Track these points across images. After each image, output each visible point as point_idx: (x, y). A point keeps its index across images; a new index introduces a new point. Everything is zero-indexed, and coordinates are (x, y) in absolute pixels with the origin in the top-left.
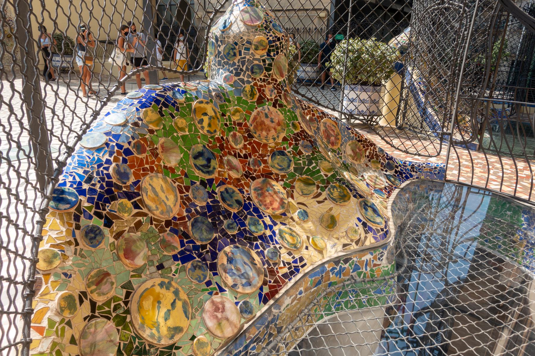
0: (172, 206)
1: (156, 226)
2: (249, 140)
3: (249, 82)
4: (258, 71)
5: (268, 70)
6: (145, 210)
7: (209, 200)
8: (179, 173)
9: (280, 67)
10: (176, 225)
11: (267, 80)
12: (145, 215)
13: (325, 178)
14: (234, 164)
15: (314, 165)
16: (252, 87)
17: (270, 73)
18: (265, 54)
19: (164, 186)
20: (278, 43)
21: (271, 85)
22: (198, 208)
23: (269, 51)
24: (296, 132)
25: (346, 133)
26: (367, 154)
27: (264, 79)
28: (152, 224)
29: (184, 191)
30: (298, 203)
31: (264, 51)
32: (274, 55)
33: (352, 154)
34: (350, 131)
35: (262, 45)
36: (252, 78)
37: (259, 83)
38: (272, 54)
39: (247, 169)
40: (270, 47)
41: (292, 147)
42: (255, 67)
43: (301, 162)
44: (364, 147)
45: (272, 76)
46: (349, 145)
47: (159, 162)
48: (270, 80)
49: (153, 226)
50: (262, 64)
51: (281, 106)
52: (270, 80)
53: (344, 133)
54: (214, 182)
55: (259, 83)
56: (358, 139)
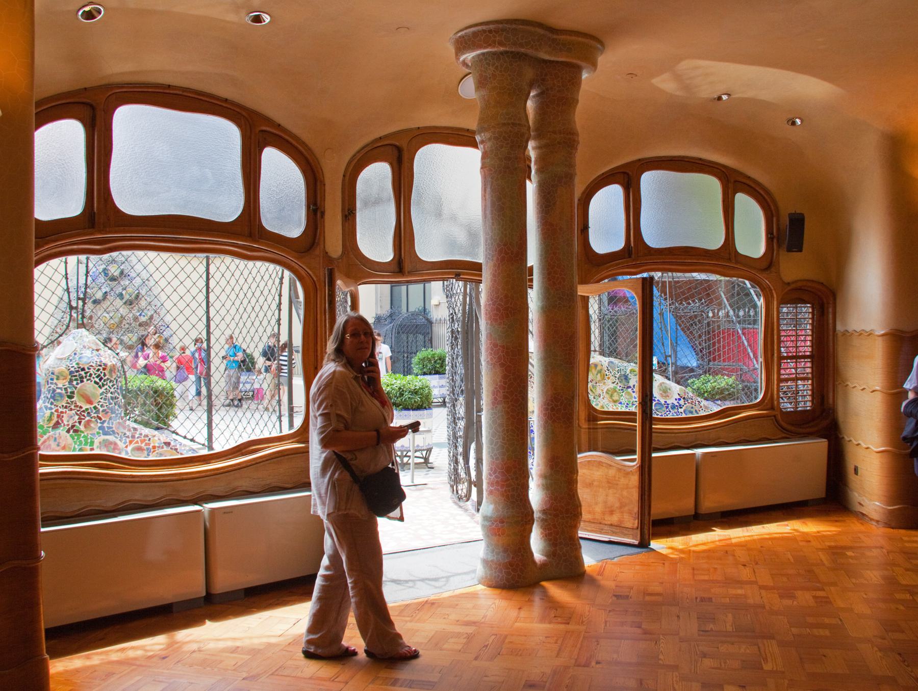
16: (52, 413)
20: (83, 373)
37: (60, 410)
38: (75, 383)
50: (64, 392)
51: (76, 431)
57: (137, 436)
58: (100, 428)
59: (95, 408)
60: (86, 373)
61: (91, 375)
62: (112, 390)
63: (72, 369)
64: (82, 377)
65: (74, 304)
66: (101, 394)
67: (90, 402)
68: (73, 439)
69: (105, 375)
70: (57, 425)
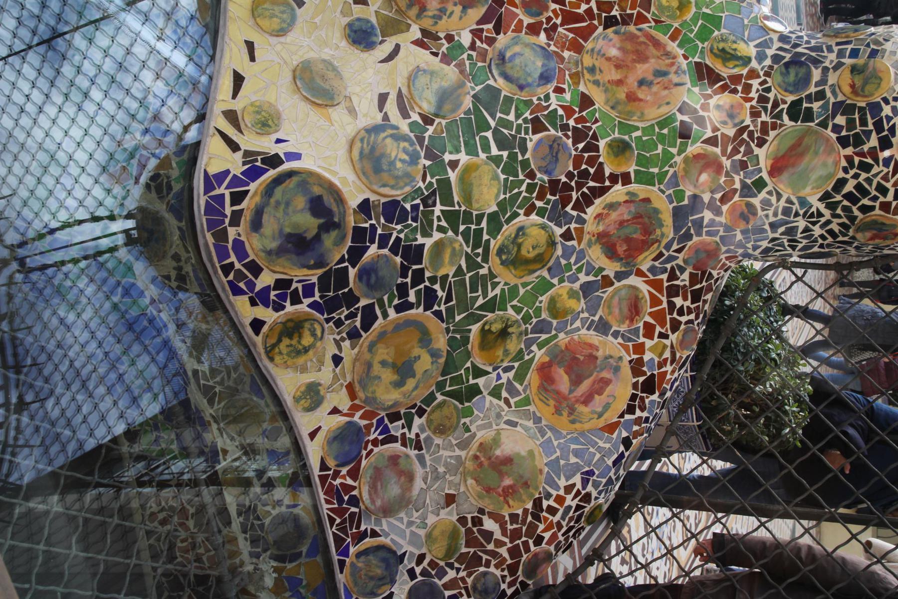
2: (600, 16)
3: (761, 57)
4: (792, 78)
5: (795, 111)
9: (801, 155)
11: (765, 109)
13: (447, 157)
15: (495, 151)
16: (747, 60)
17: (785, 117)
18: (840, 98)
20: (874, 142)
21: (748, 121)
24: (602, 144)
25: (573, 460)
26: (489, 524)
27: (767, 100)
30: (397, 48)
31: (847, 89)
32: (837, 129)
33: (498, 452)
34: (577, 479)
35: (866, 82)
36: (771, 67)
37: (755, 83)
38: (840, 120)
40: (861, 109)
41: (560, 112)
42: (803, 71)
43: (511, 117)
44: (514, 518)
45: (774, 127)
48: (764, 118)
50: (813, 89)
52: (764, 118)
53: (576, 453)
55: (755, 83)
56: (545, 504)
57: (678, 301)
59: (760, 184)
60: (873, 153)
61: (866, 167)
62: (817, 231)
64: (858, 141)
66: (803, 202)
67: (775, 171)
68: (662, 124)
69: (865, 209)
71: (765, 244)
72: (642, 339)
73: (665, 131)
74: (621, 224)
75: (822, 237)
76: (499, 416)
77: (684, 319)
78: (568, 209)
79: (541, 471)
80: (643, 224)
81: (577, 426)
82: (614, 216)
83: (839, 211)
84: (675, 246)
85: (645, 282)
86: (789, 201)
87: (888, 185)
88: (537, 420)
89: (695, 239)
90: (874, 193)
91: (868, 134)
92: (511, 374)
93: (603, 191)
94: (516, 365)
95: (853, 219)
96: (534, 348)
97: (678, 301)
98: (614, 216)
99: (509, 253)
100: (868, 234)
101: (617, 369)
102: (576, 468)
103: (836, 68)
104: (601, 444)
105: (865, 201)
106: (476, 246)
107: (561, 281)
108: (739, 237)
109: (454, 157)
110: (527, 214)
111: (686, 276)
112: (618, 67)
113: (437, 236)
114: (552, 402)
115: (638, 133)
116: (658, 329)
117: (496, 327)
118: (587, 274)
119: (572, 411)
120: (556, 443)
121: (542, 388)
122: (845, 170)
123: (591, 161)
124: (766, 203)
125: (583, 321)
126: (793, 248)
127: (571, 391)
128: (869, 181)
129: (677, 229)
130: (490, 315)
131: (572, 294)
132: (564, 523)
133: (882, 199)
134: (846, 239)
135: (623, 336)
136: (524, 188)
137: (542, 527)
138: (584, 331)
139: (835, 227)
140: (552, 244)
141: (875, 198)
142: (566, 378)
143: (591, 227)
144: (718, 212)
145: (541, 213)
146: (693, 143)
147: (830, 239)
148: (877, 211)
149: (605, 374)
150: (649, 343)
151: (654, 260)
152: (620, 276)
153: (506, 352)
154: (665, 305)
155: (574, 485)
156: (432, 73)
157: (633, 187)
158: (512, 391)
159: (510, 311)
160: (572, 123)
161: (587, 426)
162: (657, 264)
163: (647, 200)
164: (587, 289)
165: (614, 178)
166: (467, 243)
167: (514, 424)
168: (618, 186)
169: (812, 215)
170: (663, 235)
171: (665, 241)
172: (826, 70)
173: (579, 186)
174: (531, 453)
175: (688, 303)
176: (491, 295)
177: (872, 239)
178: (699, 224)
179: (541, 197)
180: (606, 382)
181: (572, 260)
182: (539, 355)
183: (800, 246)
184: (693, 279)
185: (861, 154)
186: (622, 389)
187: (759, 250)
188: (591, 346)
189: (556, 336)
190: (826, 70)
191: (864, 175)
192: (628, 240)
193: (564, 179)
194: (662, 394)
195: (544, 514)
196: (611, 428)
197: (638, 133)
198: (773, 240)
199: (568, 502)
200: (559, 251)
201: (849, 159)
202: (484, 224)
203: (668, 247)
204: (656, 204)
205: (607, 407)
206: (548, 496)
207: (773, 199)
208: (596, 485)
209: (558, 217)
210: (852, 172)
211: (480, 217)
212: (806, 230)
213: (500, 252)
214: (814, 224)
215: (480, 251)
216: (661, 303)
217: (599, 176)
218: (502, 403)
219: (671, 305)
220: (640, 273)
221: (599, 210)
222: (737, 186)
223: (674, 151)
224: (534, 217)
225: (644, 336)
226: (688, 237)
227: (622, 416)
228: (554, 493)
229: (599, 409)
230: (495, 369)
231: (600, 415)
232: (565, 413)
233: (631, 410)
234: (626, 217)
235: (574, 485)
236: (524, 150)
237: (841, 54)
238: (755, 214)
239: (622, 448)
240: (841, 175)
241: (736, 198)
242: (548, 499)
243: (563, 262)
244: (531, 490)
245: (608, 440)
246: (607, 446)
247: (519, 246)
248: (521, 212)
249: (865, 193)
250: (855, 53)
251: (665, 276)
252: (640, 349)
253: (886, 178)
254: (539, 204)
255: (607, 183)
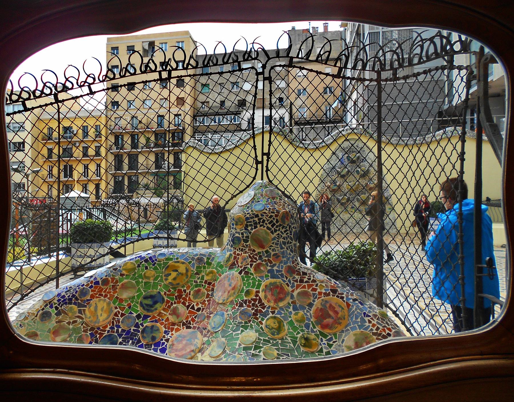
0: (101, 320)
1: (84, 327)
3: (231, 251)
4: (237, 242)
6: (83, 316)
7: (133, 328)
8: (126, 304)
10: (97, 332)
12: (82, 318)
13: (237, 347)
14: (180, 311)
15: (240, 332)
16: (231, 255)
19: (105, 307)
20: (256, 219)
21: (247, 255)
22: (120, 330)
23: (247, 226)
24: (245, 298)
27: (242, 249)
28: (82, 325)
29: (119, 316)
31: (242, 226)
32: (252, 229)
34: (367, 319)
35: (240, 221)
37: (237, 252)
38: (249, 228)
39: (190, 319)
41: (233, 311)
42: (236, 239)
43: (231, 326)
46: (355, 335)
47: (114, 293)
49: (82, 327)
50: (241, 236)
51: (247, 273)
52: (247, 250)
53: (356, 318)
54: (149, 319)
55: (237, 252)
57: (305, 280)
58: (269, 271)
59: (267, 252)
60: (259, 219)
61: (264, 221)
62: (285, 235)
63: (248, 216)
64: (256, 223)
65: (259, 159)
66: (274, 239)
67: (263, 247)
68: (243, 280)
69: (277, 221)
70: (232, 266)
71: (289, 251)
72: (317, 292)
73: (246, 279)
74: (272, 295)
75: (287, 234)
76: (340, 346)
77: (312, 278)
78: (263, 311)
79: (362, 332)
80: (274, 288)
81: (346, 317)
82: (269, 297)
83: (277, 229)
84: (285, 279)
85: (297, 289)
86: (273, 243)
87: (269, 215)
88: (343, 331)
89: (283, 272)
90: (272, 219)
91: (254, 221)
92: (324, 339)
93: (260, 300)
94: (320, 337)
95: (280, 225)
96: (315, 330)
97: (305, 280)
98: (269, 297)
99: (274, 332)
100: (286, 221)
101: (326, 302)
102: (362, 319)
103: (236, 230)
104: (354, 309)
105: (275, 221)
106: (269, 342)
107: (290, 317)
108: (285, 259)
109: (238, 345)
110: (262, 324)
111: (297, 277)
112: (225, 292)
113: (261, 354)
114: (336, 325)
115: (245, 287)
116: (314, 287)
117: (303, 341)
118: (290, 308)
119: (340, 318)
120: (352, 326)
121: (330, 328)
122: (264, 227)
123: (250, 302)
124: (273, 250)
125: (307, 311)
126: (291, 243)
127: (333, 318)
128: (268, 220)
129: (279, 278)
130: (298, 343)
131: (296, 314)
132: (384, 325)
133: (274, 217)
134: (288, 227)
135: (315, 298)
136: (253, 324)
137: (384, 333)
138: (311, 312)
139: (283, 230)
140: (275, 318)
141: (274, 219)
142: (327, 320)
143: (272, 304)
144: (275, 265)
145: (263, 319)
146: (250, 270)
147: (288, 232)
148: (278, 218)
149: (328, 305)
150: (319, 290)
151: (288, 286)
152: (292, 297)
153: (314, 339)
154: (306, 284)
155: (369, 320)
156: (212, 350)
157: (261, 290)
158: (331, 339)
159: (299, 336)
160: (237, 307)
161: (346, 313)
162: (290, 286)
163: (266, 286)
164: (295, 309)
165: (257, 296)
166: (267, 344)
167: (343, 340)
168: (260, 295)
169: (279, 237)
170: (279, 282)
171: (282, 282)
172: (236, 232)
173: (257, 306)
174: (355, 335)
175: (307, 277)
176: (290, 341)
177: (288, 220)
178: (278, 271)
179: (257, 319)
180: (331, 305)
181: (283, 312)
182: (318, 329)
183: (290, 241)
184: (299, 274)
185: (259, 223)
186: (333, 299)
187: (291, 253)
188: (317, 310)
189: (312, 322)
190: (236, 232)
191: (266, 222)
192: (279, 293)
193: (254, 311)
194: (339, 287)
195: (378, 332)
196: (348, 305)
197: (245, 287)
198: (287, 249)
199: (375, 323)
200: (279, 316)
201: (261, 226)
202: (262, 338)
203: (284, 281)
204: (268, 283)
205: (340, 306)
206: (372, 330)
207: (272, 248)
208: (370, 312)
209: (265, 315)
210: (265, 225)
211: (259, 339)
212: (284, 238)
213: (273, 334)
214: (281, 236)
215: (271, 341)
216: (305, 285)
217: (255, 300)
218: (335, 344)
219: (306, 282)
220: (293, 291)
221: (266, 301)
222: (267, 259)
223: (252, 277)
224: (264, 322)
225: (316, 291)
226: (282, 275)
227: (344, 301)
228: (371, 327)
229: (341, 309)
230: (321, 345)
231: (343, 309)
232: (341, 321)
233: (342, 298)
234: (270, 293)
235: (369, 320)
236: (242, 323)
237: (233, 228)
238: (277, 254)
239: (357, 302)
240: (265, 228)
241: (271, 259)
242: (373, 330)
243: (283, 315)
244: (369, 336)
245: (353, 306)
246: (355, 307)
247: (273, 328)
248: (261, 326)
249: (272, 221)
250: (233, 225)
251: (296, 283)
252: (320, 293)
253: (267, 216)
254: (260, 320)
255: (258, 298)
